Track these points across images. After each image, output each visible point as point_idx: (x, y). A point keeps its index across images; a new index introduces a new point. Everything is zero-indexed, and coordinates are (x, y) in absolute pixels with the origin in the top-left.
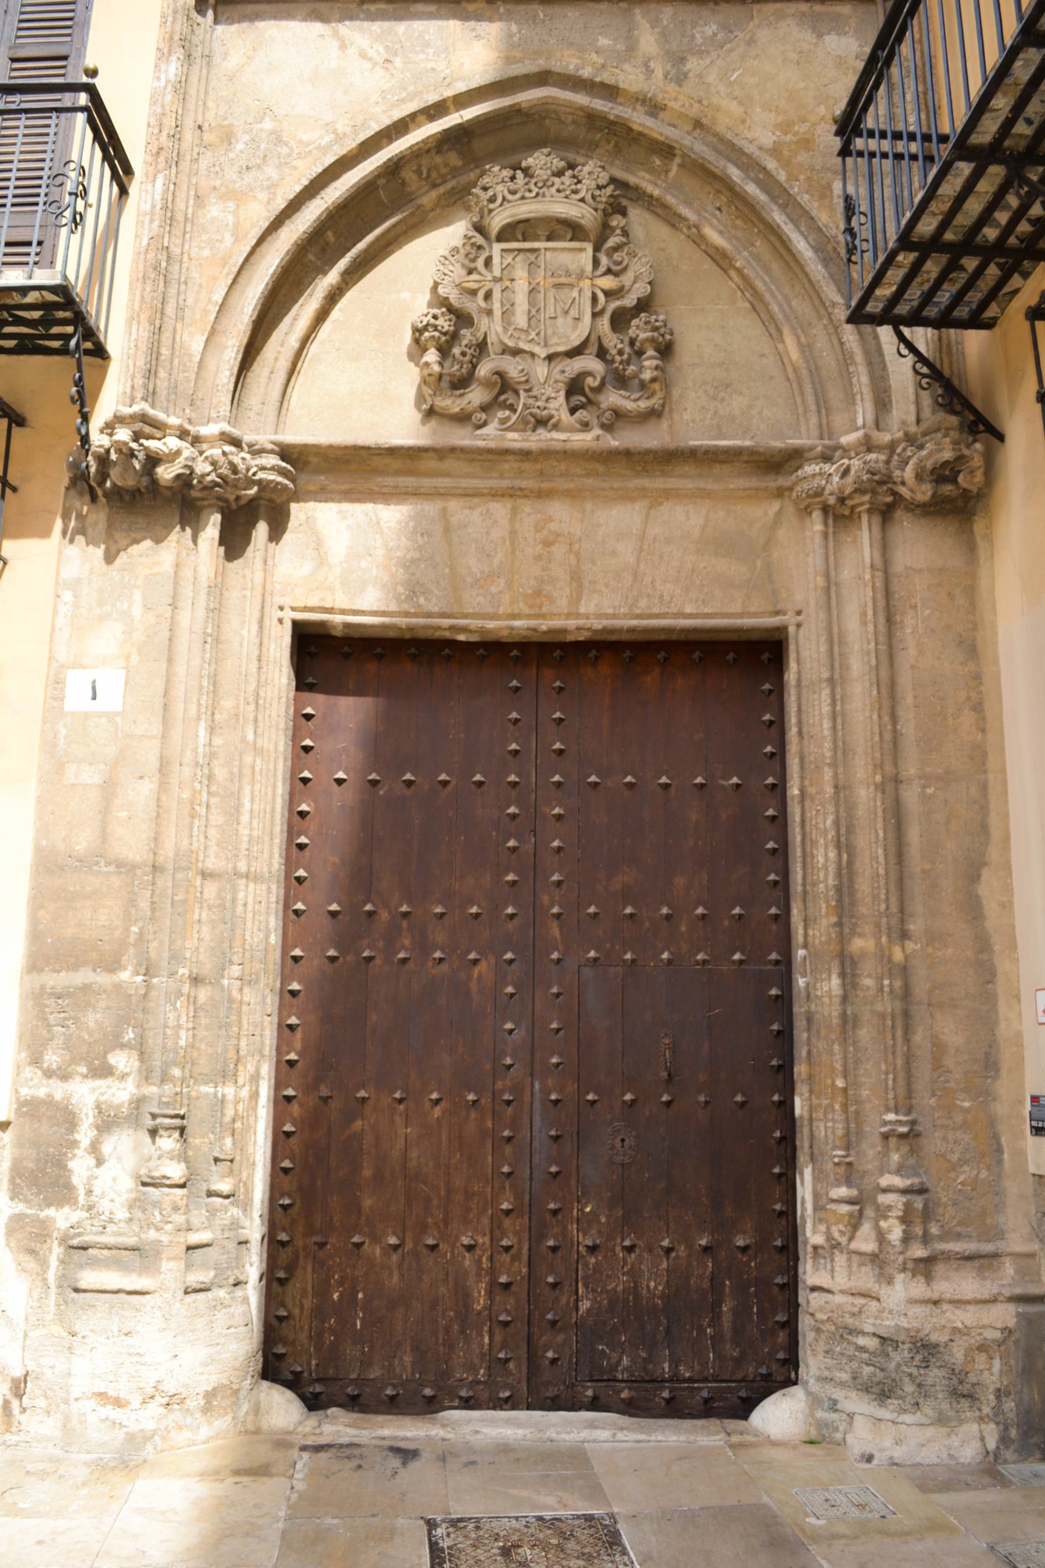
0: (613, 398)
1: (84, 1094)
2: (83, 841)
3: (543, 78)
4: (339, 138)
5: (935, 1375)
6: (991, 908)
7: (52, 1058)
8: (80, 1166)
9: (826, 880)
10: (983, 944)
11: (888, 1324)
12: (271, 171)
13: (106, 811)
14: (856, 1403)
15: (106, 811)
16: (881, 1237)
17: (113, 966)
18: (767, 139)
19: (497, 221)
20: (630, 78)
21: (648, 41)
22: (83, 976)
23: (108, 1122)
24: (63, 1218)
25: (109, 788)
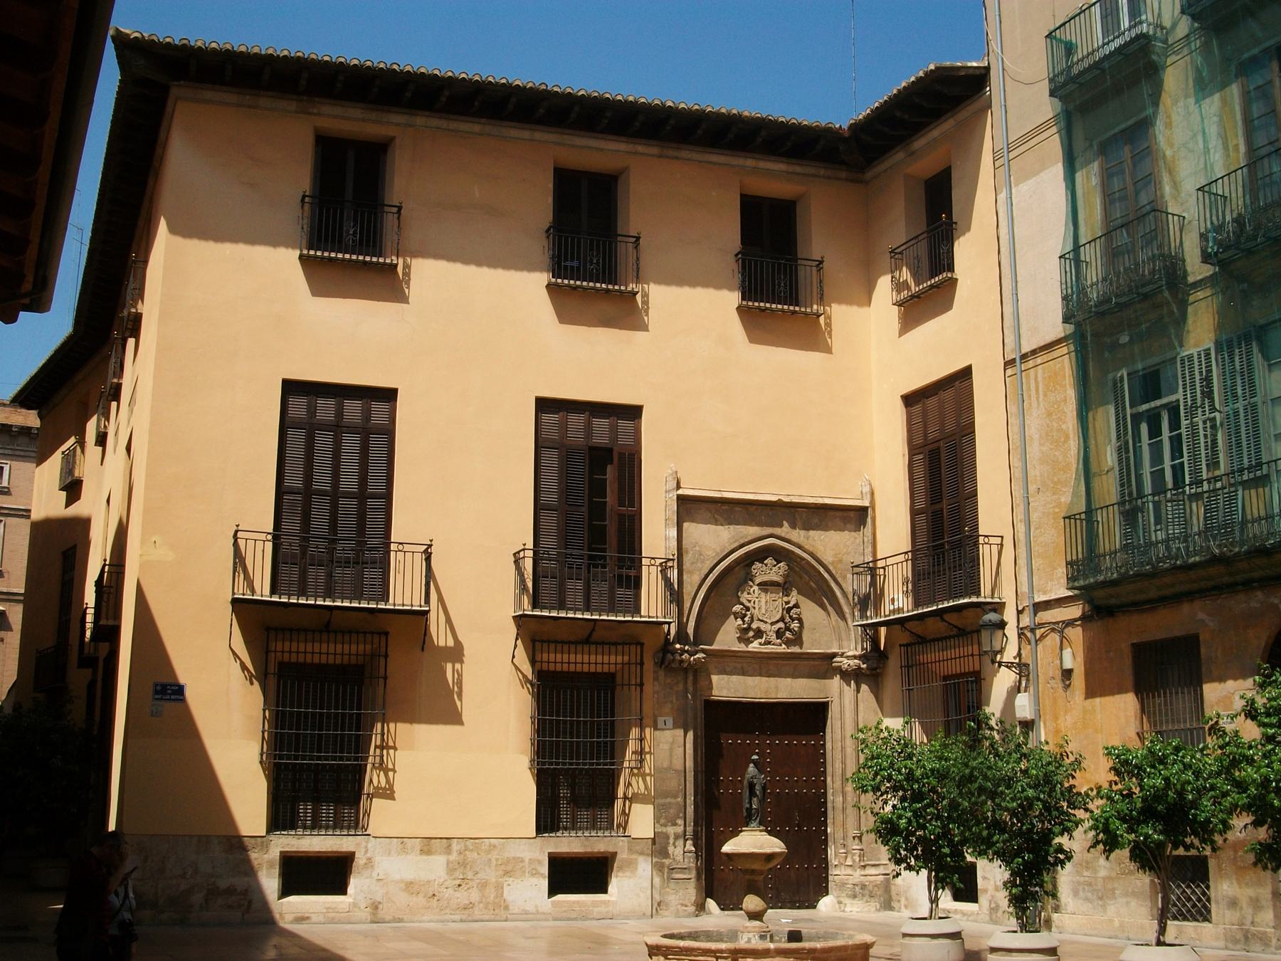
0: (788, 634)
1: (671, 830)
2: (666, 765)
5: (867, 892)
7: (662, 821)
8: (671, 849)
11: (855, 881)
13: (671, 756)
14: (847, 901)
15: (671, 756)
16: (854, 861)
17: (676, 797)
18: (831, 560)
19: (758, 580)
22: (669, 800)
23: (677, 837)
24: (667, 861)
25: (671, 750)
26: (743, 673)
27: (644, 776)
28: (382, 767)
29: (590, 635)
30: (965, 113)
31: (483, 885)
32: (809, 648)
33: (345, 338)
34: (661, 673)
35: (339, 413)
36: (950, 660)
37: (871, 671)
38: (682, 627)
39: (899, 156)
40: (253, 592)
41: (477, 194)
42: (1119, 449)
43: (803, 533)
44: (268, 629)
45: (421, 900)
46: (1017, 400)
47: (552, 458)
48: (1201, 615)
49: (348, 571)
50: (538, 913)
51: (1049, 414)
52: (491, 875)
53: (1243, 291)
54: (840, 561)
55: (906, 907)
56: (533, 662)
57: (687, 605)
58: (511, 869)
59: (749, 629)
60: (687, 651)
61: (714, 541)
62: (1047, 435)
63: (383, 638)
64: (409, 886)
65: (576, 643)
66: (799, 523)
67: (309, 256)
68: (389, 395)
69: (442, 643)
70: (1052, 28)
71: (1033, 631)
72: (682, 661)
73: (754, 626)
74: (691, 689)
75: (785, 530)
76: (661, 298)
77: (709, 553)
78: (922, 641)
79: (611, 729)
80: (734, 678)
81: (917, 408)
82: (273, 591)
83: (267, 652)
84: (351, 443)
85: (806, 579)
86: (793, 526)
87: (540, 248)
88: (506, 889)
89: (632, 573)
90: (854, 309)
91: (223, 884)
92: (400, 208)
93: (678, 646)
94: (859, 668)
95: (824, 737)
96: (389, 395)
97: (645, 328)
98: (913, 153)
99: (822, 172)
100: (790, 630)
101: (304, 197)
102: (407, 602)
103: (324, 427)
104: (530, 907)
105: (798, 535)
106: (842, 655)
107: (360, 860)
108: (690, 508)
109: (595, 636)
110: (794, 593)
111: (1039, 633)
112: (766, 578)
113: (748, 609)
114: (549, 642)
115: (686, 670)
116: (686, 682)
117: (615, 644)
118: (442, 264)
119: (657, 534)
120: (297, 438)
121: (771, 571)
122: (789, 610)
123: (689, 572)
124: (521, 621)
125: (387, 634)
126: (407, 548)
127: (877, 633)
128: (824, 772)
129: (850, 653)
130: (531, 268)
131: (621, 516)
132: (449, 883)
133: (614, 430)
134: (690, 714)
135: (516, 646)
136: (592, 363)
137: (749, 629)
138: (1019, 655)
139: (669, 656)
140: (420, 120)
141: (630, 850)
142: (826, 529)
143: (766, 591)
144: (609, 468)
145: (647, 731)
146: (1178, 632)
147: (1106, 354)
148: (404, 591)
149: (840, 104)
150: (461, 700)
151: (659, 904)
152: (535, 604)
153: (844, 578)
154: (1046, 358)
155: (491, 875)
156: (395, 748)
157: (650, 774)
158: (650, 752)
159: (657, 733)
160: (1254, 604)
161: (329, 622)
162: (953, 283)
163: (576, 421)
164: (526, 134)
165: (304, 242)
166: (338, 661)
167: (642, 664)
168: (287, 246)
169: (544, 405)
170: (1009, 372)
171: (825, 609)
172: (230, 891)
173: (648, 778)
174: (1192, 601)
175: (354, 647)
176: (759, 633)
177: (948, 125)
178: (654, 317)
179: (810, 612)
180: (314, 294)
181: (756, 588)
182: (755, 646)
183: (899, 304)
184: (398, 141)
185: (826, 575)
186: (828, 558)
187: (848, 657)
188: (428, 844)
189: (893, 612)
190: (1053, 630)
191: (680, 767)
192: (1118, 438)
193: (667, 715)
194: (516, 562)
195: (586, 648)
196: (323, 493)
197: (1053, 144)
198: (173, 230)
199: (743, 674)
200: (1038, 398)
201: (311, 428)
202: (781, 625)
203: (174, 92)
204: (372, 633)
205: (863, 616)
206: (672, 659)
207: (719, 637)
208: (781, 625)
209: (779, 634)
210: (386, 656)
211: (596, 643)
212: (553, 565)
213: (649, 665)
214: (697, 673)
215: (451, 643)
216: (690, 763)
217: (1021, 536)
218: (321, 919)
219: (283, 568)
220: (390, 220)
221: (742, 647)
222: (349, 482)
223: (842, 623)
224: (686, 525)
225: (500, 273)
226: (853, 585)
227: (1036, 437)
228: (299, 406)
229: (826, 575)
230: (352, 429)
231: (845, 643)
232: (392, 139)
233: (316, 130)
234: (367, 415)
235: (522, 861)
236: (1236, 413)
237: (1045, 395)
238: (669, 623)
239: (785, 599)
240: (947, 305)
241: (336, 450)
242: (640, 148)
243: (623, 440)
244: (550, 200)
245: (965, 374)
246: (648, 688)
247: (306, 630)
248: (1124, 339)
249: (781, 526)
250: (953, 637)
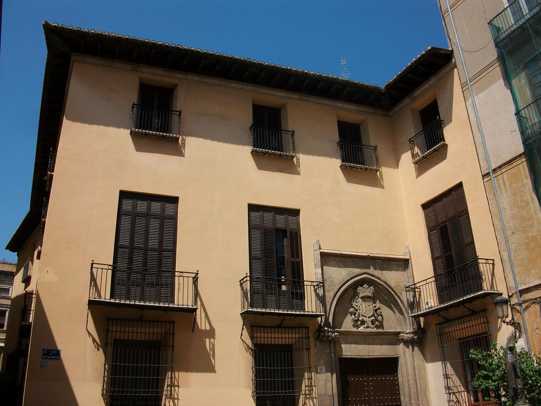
4: (341, 282)
6: (428, 396)
9: (407, 393)
10: (428, 401)
12: (332, 287)
18: (394, 285)
19: (361, 295)
25: (325, 384)
26: (357, 343)
27: (312, 399)
28: (171, 397)
29: (281, 323)
30: (440, 74)
32: (387, 329)
33: (152, 172)
34: (318, 343)
35: (149, 208)
36: (470, 328)
37: (419, 341)
38: (327, 319)
39: (407, 100)
40: (100, 296)
43: (380, 272)
46: (492, 193)
47: (257, 234)
49: (153, 289)
51: (514, 194)
54: (398, 286)
56: (252, 338)
57: (328, 308)
59: (358, 320)
60: (330, 331)
61: (339, 275)
62: (514, 205)
66: (378, 267)
67: (135, 132)
68: (174, 200)
69: (203, 328)
70: (491, 18)
71: (520, 305)
72: (328, 336)
74: (333, 351)
75: (371, 270)
76: (304, 160)
77: (337, 281)
78: (448, 321)
79: (291, 374)
80: (353, 346)
81: (431, 209)
82: (112, 296)
83: (107, 332)
84: (154, 224)
85: (384, 295)
86: (375, 269)
87: (248, 136)
89: (299, 291)
90: (392, 170)
92: (180, 112)
93: (326, 328)
94: (413, 338)
95: (397, 376)
96: (174, 200)
97: (298, 173)
98: (415, 98)
99: (371, 111)
100: (378, 322)
101: (134, 105)
102: (185, 303)
103: (141, 215)
105: (377, 273)
106: (403, 333)
108: (327, 258)
109: (285, 323)
110: (378, 302)
111: (524, 306)
112: (364, 294)
113: (357, 310)
114: (260, 327)
115: (330, 342)
116: (330, 348)
117: (295, 328)
118: (201, 140)
119: (311, 270)
120: (126, 221)
121: (366, 291)
122: (376, 310)
123: (328, 291)
124: (245, 315)
125: (173, 322)
126: (185, 274)
127: (419, 320)
128: (399, 393)
129: (408, 331)
130: (243, 144)
131: (293, 263)
133: (287, 221)
135: (243, 330)
136: (274, 188)
137: (358, 320)
138: (513, 319)
139: (322, 334)
140: (190, 77)
142: (390, 270)
143: (365, 301)
144: (285, 240)
145: (313, 374)
148: (183, 298)
150: (214, 359)
152: (252, 306)
153: (401, 294)
154: (507, 168)
156: (179, 387)
157: (315, 398)
158: (315, 386)
159: (318, 375)
161: (142, 315)
162: (445, 146)
163: (268, 216)
164: (239, 86)
165: (133, 125)
167: (308, 338)
168: (124, 128)
169: (252, 208)
170: (486, 180)
171: (392, 310)
173: (315, 400)
176: (363, 322)
177: (433, 81)
178: (302, 169)
179: (385, 311)
180: (137, 151)
181: (360, 299)
182: (361, 329)
183: (415, 163)
185: (393, 293)
186: (393, 284)
187: (407, 333)
189: (429, 308)
190: (534, 303)
191: (330, 393)
193: (322, 365)
194: (241, 285)
196: (140, 248)
197: (497, 71)
198: (67, 119)
199: (357, 344)
200: (505, 189)
201: (134, 215)
202: (373, 318)
203: (73, 58)
205: (412, 313)
206: (322, 334)
207: (344, 325)
208: (373, 318)
209: (373, 322)
210: (173, 334)
211: (286, 328)
213: (312, 340)
214: (334, 343)
215: (208, 328)
216: (335, 391)
217: (505, 258)
219: (117, 287)
220: (175, 118)
221: (355, 330)
222: (153, 243)
223: (401, 317)
224: (325, 267)
225: (229, 145)
226: (406, 297)
227: (508, 207)
228: (128, 205)
229: (393, 293)
230: (156, 217)
231: (404, 327)
233: (140, 79)
234: (163, 210)
237: (510, 186)
238: (321, 316)
239: (374, 305)
240: (444, 157)
241: (147, 228)
242: (291, 95)
243: (292, 226)
246: (312, 351)
247: (129, 320)
249: (370, 268)
250: (468, 316)
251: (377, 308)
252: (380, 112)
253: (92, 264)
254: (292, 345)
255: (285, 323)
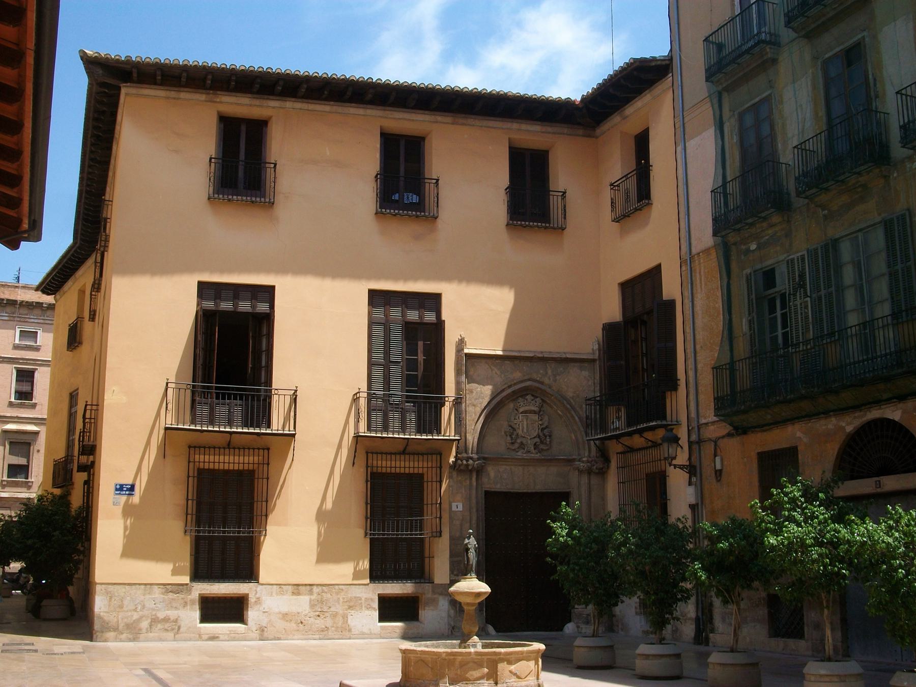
0: (542, 446)
3: (529, 380)
14: (583, 626)
19: (521, 410)
20: (546, 381)
21: (550, 372)
25: (461, 525)
31: (335, 615)
34: (455, 474)
39: (616, 119)
41: (328, 154)
42: (750, 321)
44: (190, 447)
45: (293, 625)
48: (799, 434)
50: (371, 634)
52: (339, 609)
53: (825, 216)
55: (622, 630)
58: (353, 604)
63: (266, 451)
64: (285, 616)
65: (395, 454)
70: (707, 35)
73: (519, 441)
74: (475, 484)
88: (350, 618)
91: (161, 615)
92: (275, 165)
101: (211, 159)
104: (366, 630)
107: (252, 599)
109: (409, 449)
112: (527, 408)
113: (514, 429)
115: (471, 471)
116: (471, 479)
125: (268, 449)
132: (312, 614)
134: (474, 501)
140: (290, 104)
141: (434, 592)
146: (785, 445)
147: (743, 257)
149: (572, 85)
151: (453, 628)
153: (581, 407)
155: (339, 609)
160: (830, 426)
164: (361, 111)
166: (236, 468)
172: (166, 620)
174: (793, 424)
175: (246, 458)
184: (274, 119)
186: (570, 394)
187: (583, 462)
188: (297, 588)
192: (749, 314)
195: (403, 457)
203: (123, 91)
204: (259, 449)
210: (268, 464)
211: (409, 454)
212: (380, 402)
218: (226, 637)
220: (270, 172)
227: (700, 312)
232: (271, 117)
233: (219, 113)
235: (361, 599)
236: (820, 298)
237: (706, 284)
242: (439, 118)
244: (378, 156)
245: (657, 269)
248: (753, 247)
251: (544, 426)
252: (581, 132)
253: (167, 384)
254: (422, 475)
255: (409, 449)
